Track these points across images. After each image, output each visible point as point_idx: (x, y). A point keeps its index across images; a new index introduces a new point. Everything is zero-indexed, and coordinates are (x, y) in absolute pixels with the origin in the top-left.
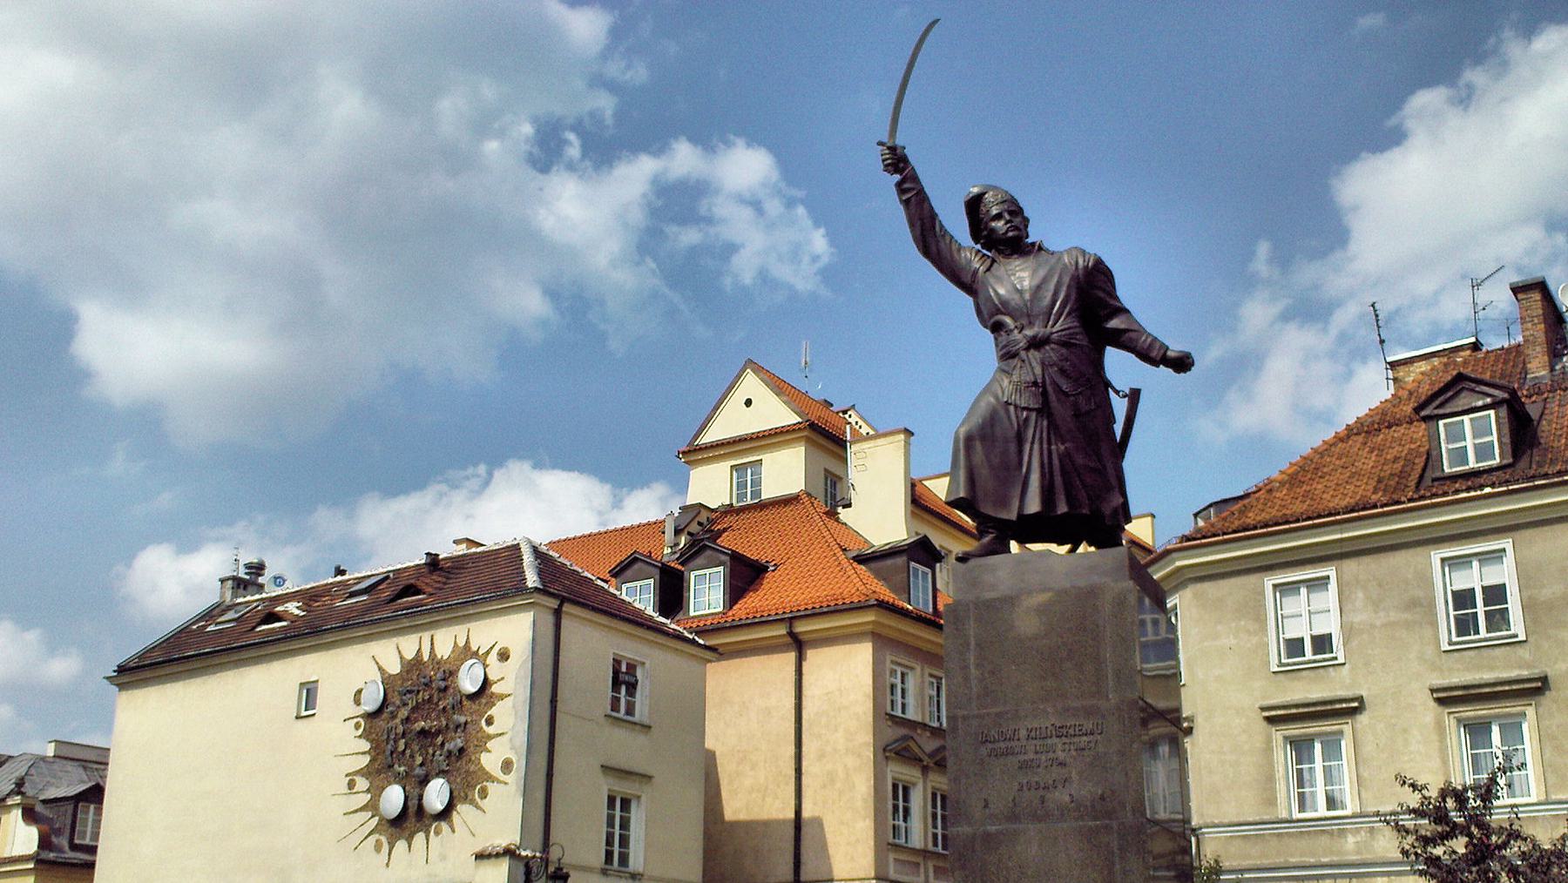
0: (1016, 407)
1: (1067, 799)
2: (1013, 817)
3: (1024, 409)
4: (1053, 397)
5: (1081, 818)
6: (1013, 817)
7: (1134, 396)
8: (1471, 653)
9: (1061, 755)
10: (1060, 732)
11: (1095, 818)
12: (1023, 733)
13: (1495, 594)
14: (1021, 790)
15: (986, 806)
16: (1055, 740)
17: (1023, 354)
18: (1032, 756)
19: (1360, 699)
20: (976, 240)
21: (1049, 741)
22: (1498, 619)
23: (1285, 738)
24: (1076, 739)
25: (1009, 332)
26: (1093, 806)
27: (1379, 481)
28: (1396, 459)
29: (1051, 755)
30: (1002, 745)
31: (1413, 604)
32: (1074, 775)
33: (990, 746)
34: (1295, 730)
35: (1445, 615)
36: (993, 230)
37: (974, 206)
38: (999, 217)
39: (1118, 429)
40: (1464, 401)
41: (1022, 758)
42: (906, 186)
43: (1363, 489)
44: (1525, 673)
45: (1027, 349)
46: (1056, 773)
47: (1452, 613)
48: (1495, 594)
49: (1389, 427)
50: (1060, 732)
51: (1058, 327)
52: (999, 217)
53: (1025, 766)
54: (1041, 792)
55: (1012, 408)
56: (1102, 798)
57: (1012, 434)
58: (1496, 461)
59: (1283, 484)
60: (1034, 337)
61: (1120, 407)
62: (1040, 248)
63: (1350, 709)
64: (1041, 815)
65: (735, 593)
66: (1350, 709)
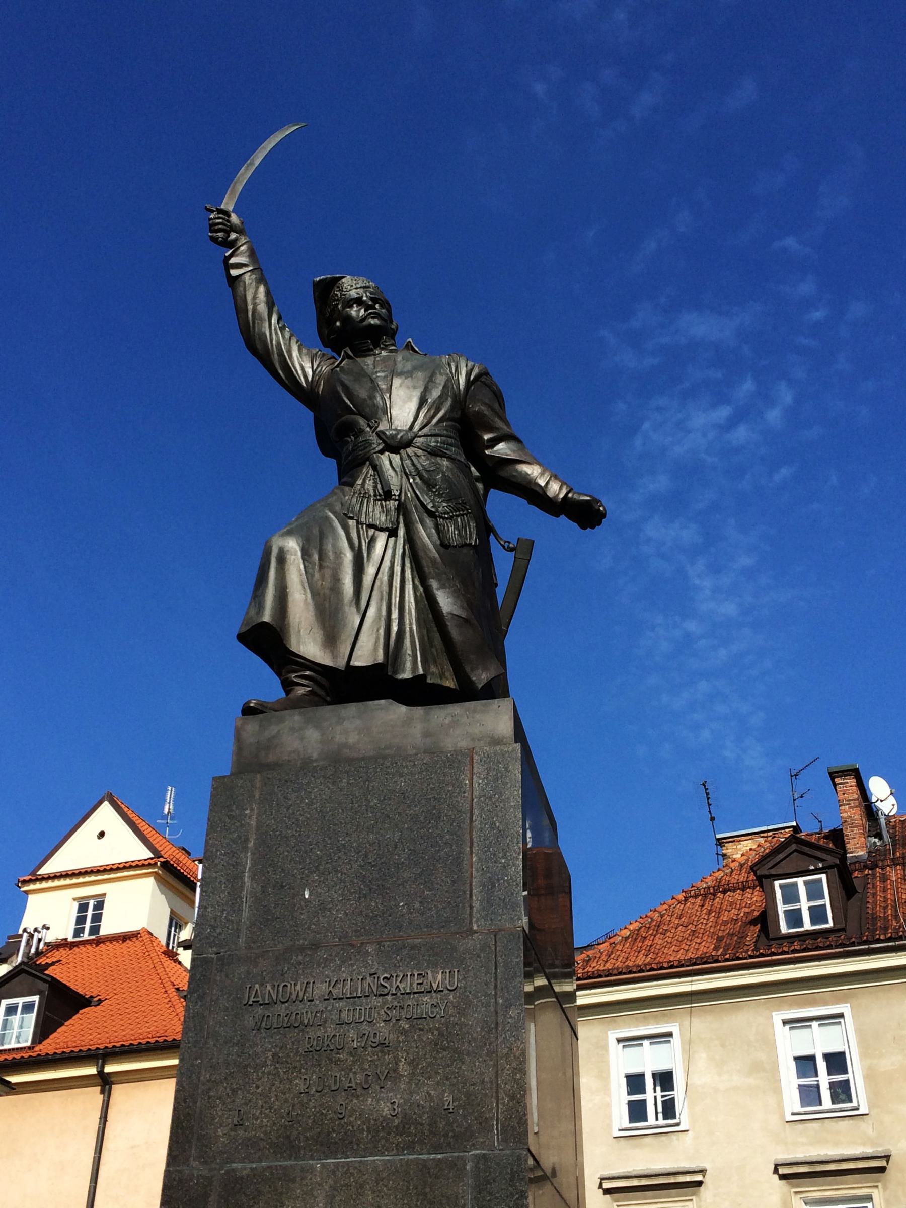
0: (358, 523)
2: (287, 1145)
3: (370, 526)
5: (410, 1147)
6: (287, 1145)
7: (523, 551)
8: (815, 1125)
9: (383, 1031)
11: (437, 1149)
13: (837, 1062)
18: (330, 1030)
19: (702, 1171)
22: (841, 1092)
26: (433, 1123)
27: (720, 939)
31: (756, 1068)
33: (260, 1010)
35: (790, 1080)
36: (349, 317)
39: (500, 593)
43: (706, 947)
44: (869, 1150)
45: (382, 452)
48: (837, 1062)
49: (724, 892)
55: (352, 523)
61: (503, 564)
65: (43, 1031)
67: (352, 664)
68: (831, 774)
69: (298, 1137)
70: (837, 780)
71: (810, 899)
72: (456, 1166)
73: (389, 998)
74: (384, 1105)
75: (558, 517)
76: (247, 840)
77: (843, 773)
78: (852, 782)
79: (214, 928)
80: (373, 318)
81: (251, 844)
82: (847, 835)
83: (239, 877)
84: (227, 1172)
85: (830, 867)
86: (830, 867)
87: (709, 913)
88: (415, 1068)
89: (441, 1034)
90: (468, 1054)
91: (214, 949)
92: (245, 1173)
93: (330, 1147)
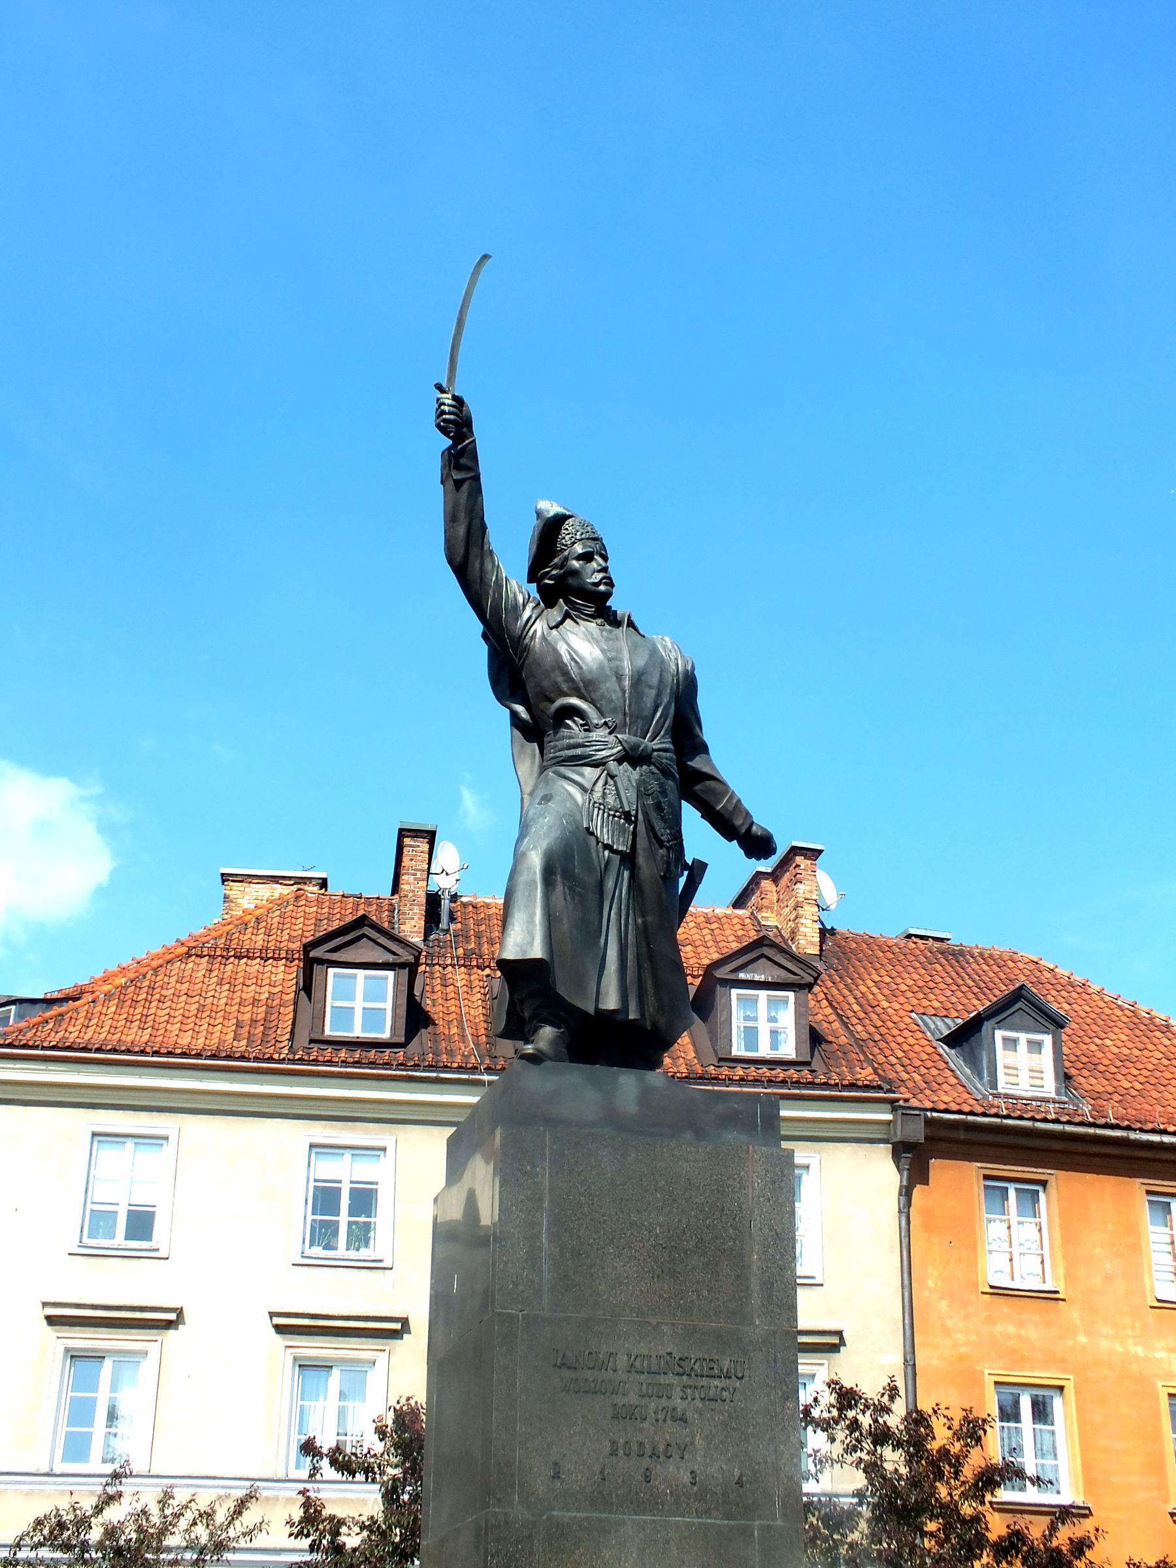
1: (686, 1478)
3: (607, 847)
4: (642, 843)
5: (707, 1513)
6: (599, 1500)
10: (681, 1366)
11: (728, 1516)
12: (622, 1361)
13: (364, 1199)
14: (614, 1453)
15: (557, 1476)
16: (671, 1379)
17: (612, 765)
18: (633, 1399)
20: (533, 575)
21: (663, 1379)
23: (67, 1350)
24: (704, 1382)
25: (588, 727)
26: (725, 1494)
28: (255, 1002)
29: (664, 1402)
30: (589, 1374)
32: (699, 1442)
33: (567, 1374)
34: (83, 1339)
37: (551, 529)
38: (587, 557)
40: (364, 952)
41: (619, 1400)
42: (463, 461)
43: (222, 1035)
45: (620, 761)
46: (672, 1431)
47: (310, 1217)
49: (240, 958)
50: (681, 1366)
51: (656, 744)
52: (587, 557)
53: (626, 1415)
54: (646, 1462)
56: (740, 1483)
57: (591, 880)
58: (386, 1035)
59: (109, 996)
60: (635, 747)
62: (631, 624)
63: (168, 1321)
64: (644, 1500)
66: (168, 1321)
67: (601, 1006)
68: (400, 830)
69: (610, 1494)
70: (407, 841)
71: (366, 999)
72: (746, 1532)
73: (685, 1378)
74: (676, 1472)
75: (730, 840)
76: (541, 1200)
77: (416, 833)
78: (426, 847)
79: (515, 1284)
80: (605, 584)
81: (546, 1204)
82: (404, 914)
83: (537, 1237)
84: (549, 1518)
85: (402, 966)
86: (402, 966)
87: (220, 983)
88: (709, 1444)
89: (730, 1416)
90: (753, 1437)
91: (519, 1306)
92: (566, 1520)
93: (640, 1507)
